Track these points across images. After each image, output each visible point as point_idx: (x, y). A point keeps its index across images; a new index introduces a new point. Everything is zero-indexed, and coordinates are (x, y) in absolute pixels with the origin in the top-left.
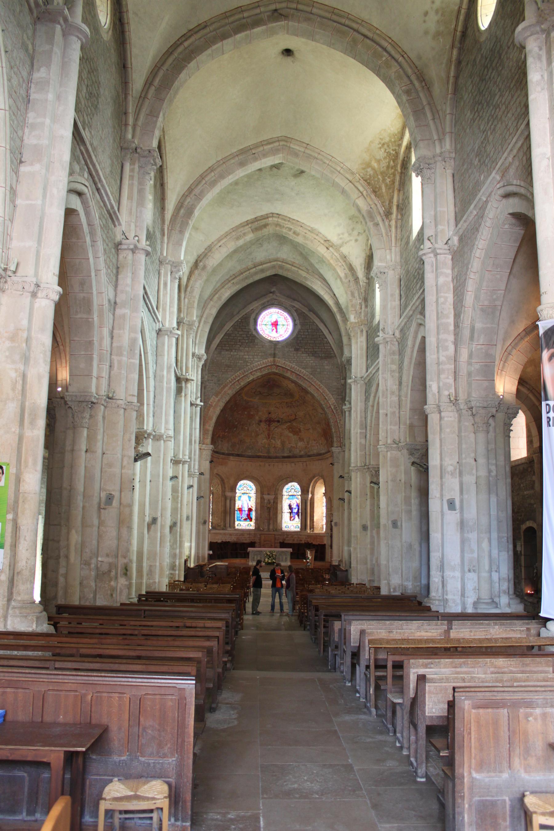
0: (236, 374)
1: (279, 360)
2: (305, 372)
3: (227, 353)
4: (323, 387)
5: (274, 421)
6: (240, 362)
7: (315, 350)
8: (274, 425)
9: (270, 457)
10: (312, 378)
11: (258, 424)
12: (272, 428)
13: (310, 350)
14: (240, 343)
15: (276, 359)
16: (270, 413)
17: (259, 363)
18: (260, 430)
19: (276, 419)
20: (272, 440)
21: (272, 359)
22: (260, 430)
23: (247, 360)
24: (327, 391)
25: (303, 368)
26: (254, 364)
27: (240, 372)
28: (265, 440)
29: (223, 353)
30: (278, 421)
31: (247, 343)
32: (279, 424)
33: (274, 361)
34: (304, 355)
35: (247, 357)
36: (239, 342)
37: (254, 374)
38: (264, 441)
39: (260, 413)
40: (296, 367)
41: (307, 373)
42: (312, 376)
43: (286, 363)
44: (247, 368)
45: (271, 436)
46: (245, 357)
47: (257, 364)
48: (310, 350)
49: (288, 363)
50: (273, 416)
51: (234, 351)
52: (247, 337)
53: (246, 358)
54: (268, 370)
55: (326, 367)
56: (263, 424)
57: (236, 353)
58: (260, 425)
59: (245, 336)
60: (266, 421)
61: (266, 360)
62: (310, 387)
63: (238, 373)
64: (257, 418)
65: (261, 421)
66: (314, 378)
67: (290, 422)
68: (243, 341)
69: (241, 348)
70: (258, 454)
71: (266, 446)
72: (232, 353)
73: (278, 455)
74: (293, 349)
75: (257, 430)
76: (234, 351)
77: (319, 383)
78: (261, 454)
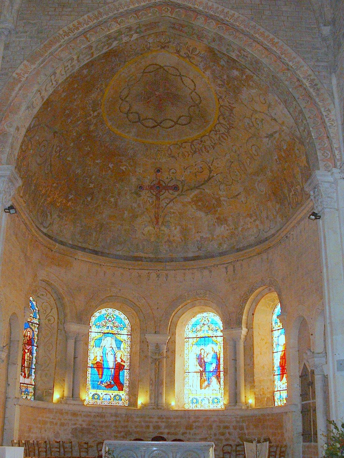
4: (281, 43)
5: (167, 188)
8: (166, 194)
9: (159, 260)
11: (137, 194)
12: (163, 203)
16: (158, 171)
20: (163, 228)
22: (139, 206)
24: (290, 50)
28: (150, 228)
30: (175, 188)
32: (176, 193)
38: (147, 229)
39: (139, 170)
41: (242, 18)
42: (253, 23)
45: (160, 220)
50: (165, 176)
58: (140, 196)
60: (151, 188)
64: (134, 180)
65: (141, 187)
70: (136, 254)
71: (152, 239)
75: (135, 205)
77: (271, 36)
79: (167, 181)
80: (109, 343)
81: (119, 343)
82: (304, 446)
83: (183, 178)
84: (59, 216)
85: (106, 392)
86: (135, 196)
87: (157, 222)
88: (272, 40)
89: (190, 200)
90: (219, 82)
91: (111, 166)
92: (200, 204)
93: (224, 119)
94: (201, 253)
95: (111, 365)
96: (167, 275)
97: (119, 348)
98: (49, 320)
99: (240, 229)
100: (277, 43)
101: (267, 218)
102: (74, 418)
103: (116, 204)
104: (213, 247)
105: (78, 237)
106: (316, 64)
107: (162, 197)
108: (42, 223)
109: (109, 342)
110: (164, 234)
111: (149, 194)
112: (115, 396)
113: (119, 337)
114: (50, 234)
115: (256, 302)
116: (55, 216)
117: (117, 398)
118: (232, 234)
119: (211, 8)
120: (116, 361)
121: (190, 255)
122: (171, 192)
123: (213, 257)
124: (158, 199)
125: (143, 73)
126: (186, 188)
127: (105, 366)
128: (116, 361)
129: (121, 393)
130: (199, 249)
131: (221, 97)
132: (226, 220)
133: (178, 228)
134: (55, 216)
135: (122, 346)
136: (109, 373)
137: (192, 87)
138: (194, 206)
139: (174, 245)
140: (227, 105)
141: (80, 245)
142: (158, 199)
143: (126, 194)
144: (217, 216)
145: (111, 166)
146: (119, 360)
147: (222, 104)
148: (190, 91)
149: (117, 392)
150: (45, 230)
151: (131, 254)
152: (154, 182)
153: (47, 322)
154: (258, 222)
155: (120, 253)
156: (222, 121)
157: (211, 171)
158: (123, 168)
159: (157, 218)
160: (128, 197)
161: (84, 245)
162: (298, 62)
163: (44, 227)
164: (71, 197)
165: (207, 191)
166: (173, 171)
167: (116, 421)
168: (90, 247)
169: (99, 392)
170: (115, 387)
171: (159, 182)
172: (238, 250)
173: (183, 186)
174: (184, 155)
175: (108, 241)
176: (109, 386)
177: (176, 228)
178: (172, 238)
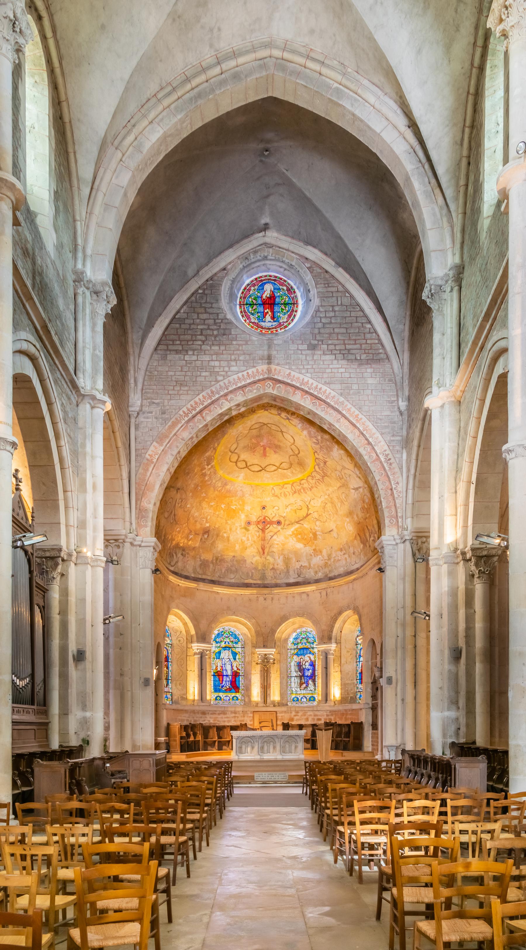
0: (197, 399)
1: (278, 368)
2: (328, 390)
3: (177, 356)
5: (271, 523)
6: (204, 374)
7: (348, 347)
9: (265, 586)
10: (342, 403)
11: (246, 529)
13: (338, 347)
14: (203, 338)
15: (273, 367)
16: (264, 508)
17: (240, 375)
18: (248, 540)
19: (275, 520)
20: (268, 557)
21: (265, 367)
22: (248, 540)
23: (217, 369)
25: (326, 383)
26: (231, 379)
27: (204, 393)
29: (169, 357)
30: (279, 523)
31: (216, 336)
32: (279, 528)
33: (269, 371)
34: (328, 357)
35: (217, 364)
36: (201, 334)
37: (232, 399)
39: (248, 508)
40: (311, 381)
41: (333, 393)
42: (342, 399)
43: (293, 373)
44: (218, 386)
45: (266, 551)
46: (212, 363)
47: (235, 377)
48: (338, 347)
49: (297, 375)
51: (190, 353)
52: (215, 324)
53: (214, 367)
54: (258, 390)
55: (370, 381)
56: (253, 528)
57: (194, 358)
58: (247, 530)
59: (211, 322)
60: (258, 523)
61: (254, 370)
62: (338, 421)
63: (201, 396)
64: (243, 516)
65: (249, 523)
66: (346, 403)
67: (297, 522)
68: (209, 332)
69: (203, 347)
70: (246, 581)
72: (187, 358)
73: (279, 581)
74: (305, 347)
75: (244, 539)
76: (190, 353)
78: (250, 581)
79: (271, 517)
80: (227, 655)
81: (235, 654)
82: (372, 733)
83: (285, 515)
84: (182, 554)
85: (226, 694)
86: (244, 530)
87: (264, 553)
88: (357, 416)
89: (291, 533)
90: (316, 441)
91: (223, 506)
92: (299, 536)
93: (319, 468)
94: (300, 580)
95: (229, 673)
96: (272, 599)
97: (235, 659)
98: (179, 641)
99: (332, 560)
100: (361, 419)
101: (354, 553)
102: (203, 716)
103: (228, 538)
104: (310, 574)
105: (198, 570)
106: (392, 439)
107: (267, 531)
108: (170, 564)
109: (226, 654)
110: (269, 563)
111: (257, 529)
112: (233, 697)
113: (234, 650)
114: (176, 571)
115: (344, 622)
116: (179, 555)
117: (235, 698)
118: (326, 565)
119: (307, 383)
120: (232, 669)
121: (292, 581)
122: (275, 526)
123: (309, 583)
124: (263, 530)
125: (250, 429)
126: (287, 523)
127: (225, 674)
128: (232, 669)
129: (238, 695)
130: (299, 576)
131: (316, 452)
132: (321, 552)
133: (281, 557)
134: (179, 555)
135: (237, 657)
136: (228, 679)
137: (292, 441)
138: (295, 539)
139: (278, 572)
140: (322, 458)
141: (200, 577)
142: (263, 530)
143: (236, 529)
144: (314, 547)
145: (223, 506)
146: (235, 669)
147: (317, 456)
148: (290, 444)
149: (233, 695)
150: (172, 569)
151: (243, 581)
152: (261, 518)
153: (178, 642)
154: (346, 556)
155: (233, 581)
156: (317, 469)
157: (308, 509)
158: (233, 507)
159: (263, 550)
160: (238, 532)
161: (204, 577)
162: (377, 438)
163: (172, 566)
164: (191, 537)
165: (305, 525)
166: (276, 508)
167: (235, 717)
168: (209, 578)
169: (221, 694)
170: (233, 690)
171: (264, 518)
172: (331, 579)
173: (285, 521)
174: (285, 495)
175: (223, 571)
176: (229, 690)
177: (279, 558)
178: (276, 566)
